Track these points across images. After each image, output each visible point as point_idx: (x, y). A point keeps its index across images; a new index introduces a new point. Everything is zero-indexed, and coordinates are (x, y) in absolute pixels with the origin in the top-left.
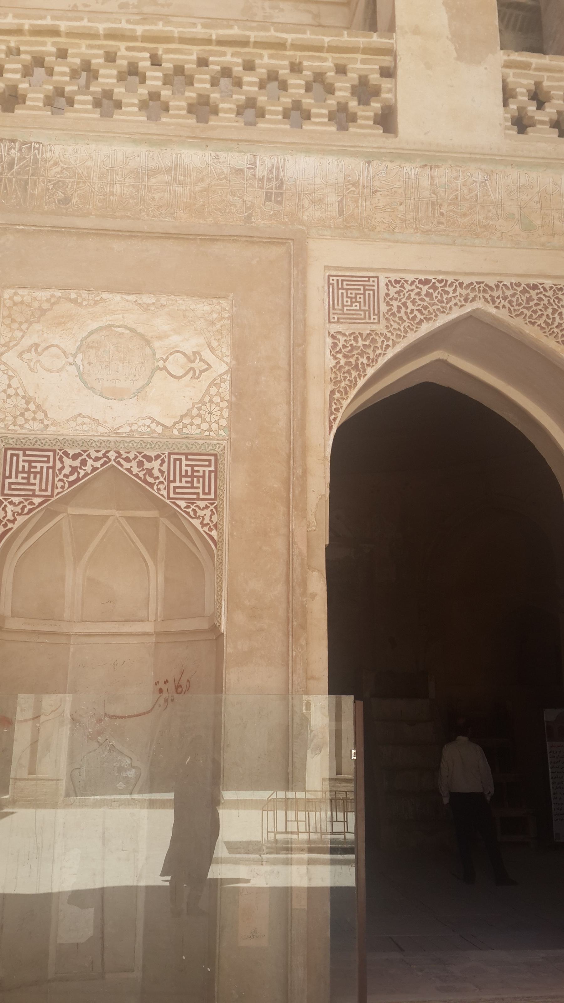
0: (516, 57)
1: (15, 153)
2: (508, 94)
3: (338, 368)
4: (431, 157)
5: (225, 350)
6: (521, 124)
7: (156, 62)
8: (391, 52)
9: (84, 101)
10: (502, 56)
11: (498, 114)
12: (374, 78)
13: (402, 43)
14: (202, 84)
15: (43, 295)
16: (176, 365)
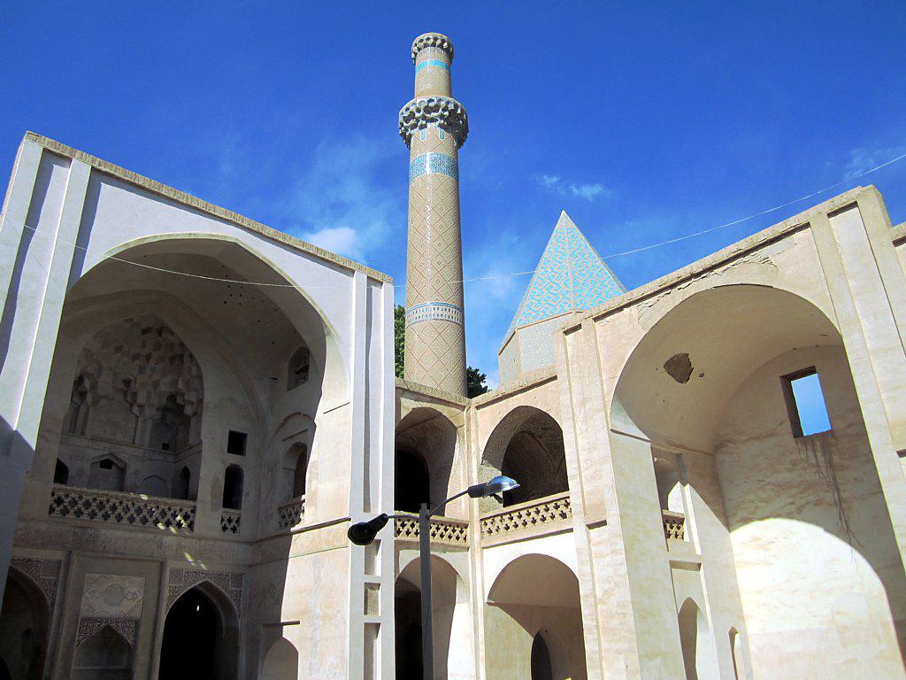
0: (226, 510)
1: (92, 532)
2: (223, 520)
3: (170, 596)
4: (200, 539)
5: (142, 592)
6: (224, 528)
7: (133, 504)
8: (195, 507)
9: (113, 517)
10: (222, 509)
11: (219, 526)
12: (189, 513)
13: (199, 505)
14: (145, 513)
15: (96, 575)
16: (130, 596)
